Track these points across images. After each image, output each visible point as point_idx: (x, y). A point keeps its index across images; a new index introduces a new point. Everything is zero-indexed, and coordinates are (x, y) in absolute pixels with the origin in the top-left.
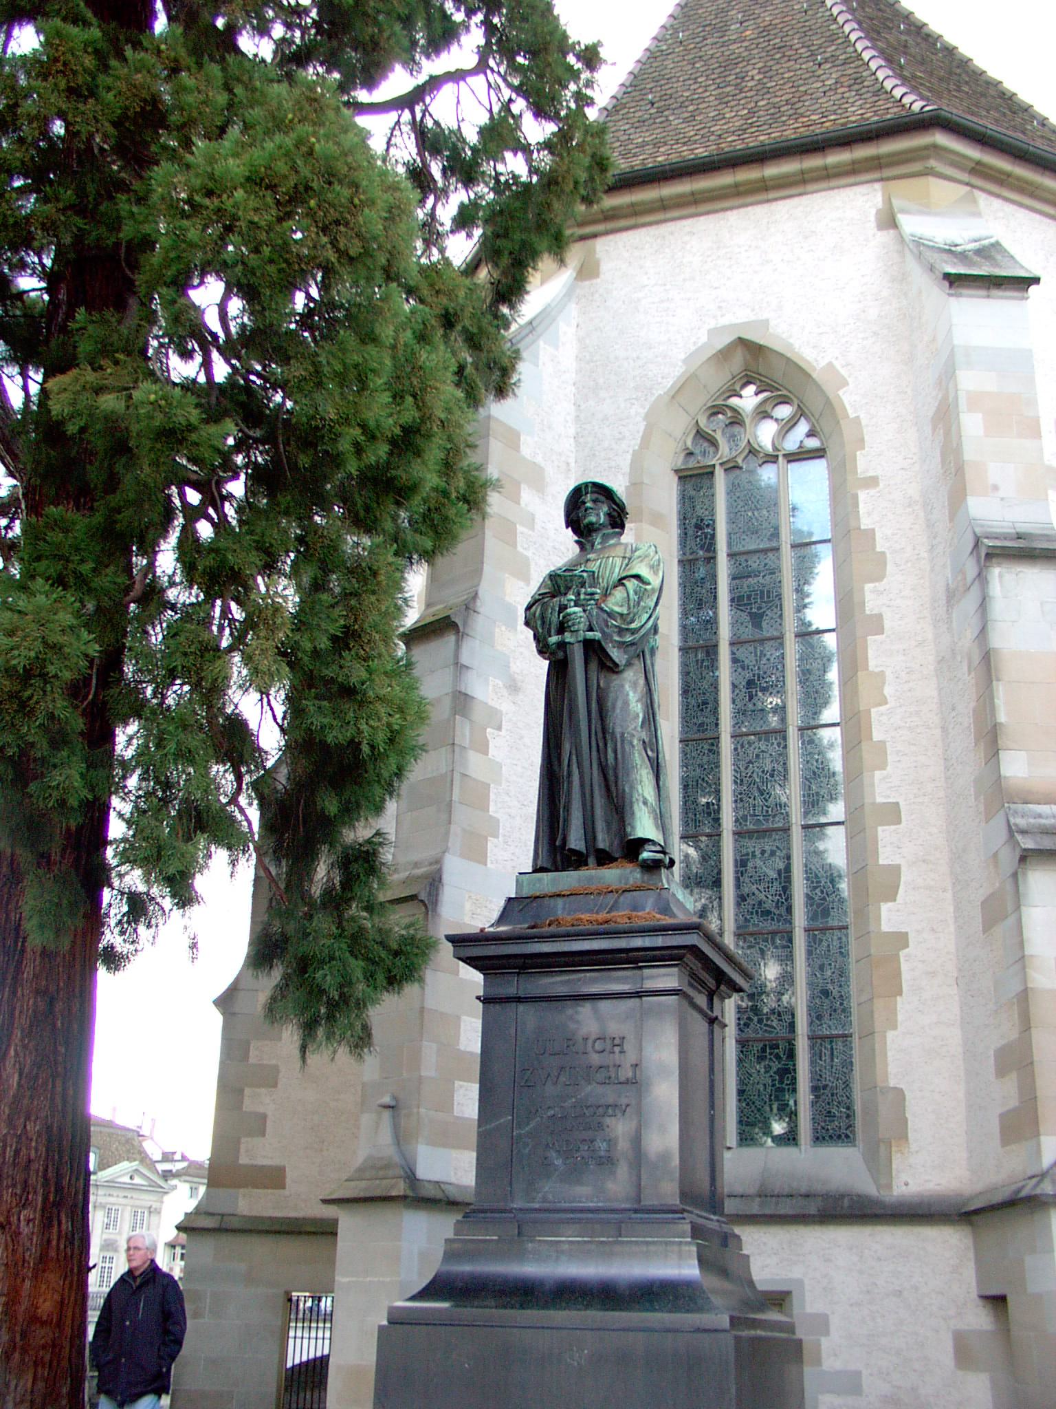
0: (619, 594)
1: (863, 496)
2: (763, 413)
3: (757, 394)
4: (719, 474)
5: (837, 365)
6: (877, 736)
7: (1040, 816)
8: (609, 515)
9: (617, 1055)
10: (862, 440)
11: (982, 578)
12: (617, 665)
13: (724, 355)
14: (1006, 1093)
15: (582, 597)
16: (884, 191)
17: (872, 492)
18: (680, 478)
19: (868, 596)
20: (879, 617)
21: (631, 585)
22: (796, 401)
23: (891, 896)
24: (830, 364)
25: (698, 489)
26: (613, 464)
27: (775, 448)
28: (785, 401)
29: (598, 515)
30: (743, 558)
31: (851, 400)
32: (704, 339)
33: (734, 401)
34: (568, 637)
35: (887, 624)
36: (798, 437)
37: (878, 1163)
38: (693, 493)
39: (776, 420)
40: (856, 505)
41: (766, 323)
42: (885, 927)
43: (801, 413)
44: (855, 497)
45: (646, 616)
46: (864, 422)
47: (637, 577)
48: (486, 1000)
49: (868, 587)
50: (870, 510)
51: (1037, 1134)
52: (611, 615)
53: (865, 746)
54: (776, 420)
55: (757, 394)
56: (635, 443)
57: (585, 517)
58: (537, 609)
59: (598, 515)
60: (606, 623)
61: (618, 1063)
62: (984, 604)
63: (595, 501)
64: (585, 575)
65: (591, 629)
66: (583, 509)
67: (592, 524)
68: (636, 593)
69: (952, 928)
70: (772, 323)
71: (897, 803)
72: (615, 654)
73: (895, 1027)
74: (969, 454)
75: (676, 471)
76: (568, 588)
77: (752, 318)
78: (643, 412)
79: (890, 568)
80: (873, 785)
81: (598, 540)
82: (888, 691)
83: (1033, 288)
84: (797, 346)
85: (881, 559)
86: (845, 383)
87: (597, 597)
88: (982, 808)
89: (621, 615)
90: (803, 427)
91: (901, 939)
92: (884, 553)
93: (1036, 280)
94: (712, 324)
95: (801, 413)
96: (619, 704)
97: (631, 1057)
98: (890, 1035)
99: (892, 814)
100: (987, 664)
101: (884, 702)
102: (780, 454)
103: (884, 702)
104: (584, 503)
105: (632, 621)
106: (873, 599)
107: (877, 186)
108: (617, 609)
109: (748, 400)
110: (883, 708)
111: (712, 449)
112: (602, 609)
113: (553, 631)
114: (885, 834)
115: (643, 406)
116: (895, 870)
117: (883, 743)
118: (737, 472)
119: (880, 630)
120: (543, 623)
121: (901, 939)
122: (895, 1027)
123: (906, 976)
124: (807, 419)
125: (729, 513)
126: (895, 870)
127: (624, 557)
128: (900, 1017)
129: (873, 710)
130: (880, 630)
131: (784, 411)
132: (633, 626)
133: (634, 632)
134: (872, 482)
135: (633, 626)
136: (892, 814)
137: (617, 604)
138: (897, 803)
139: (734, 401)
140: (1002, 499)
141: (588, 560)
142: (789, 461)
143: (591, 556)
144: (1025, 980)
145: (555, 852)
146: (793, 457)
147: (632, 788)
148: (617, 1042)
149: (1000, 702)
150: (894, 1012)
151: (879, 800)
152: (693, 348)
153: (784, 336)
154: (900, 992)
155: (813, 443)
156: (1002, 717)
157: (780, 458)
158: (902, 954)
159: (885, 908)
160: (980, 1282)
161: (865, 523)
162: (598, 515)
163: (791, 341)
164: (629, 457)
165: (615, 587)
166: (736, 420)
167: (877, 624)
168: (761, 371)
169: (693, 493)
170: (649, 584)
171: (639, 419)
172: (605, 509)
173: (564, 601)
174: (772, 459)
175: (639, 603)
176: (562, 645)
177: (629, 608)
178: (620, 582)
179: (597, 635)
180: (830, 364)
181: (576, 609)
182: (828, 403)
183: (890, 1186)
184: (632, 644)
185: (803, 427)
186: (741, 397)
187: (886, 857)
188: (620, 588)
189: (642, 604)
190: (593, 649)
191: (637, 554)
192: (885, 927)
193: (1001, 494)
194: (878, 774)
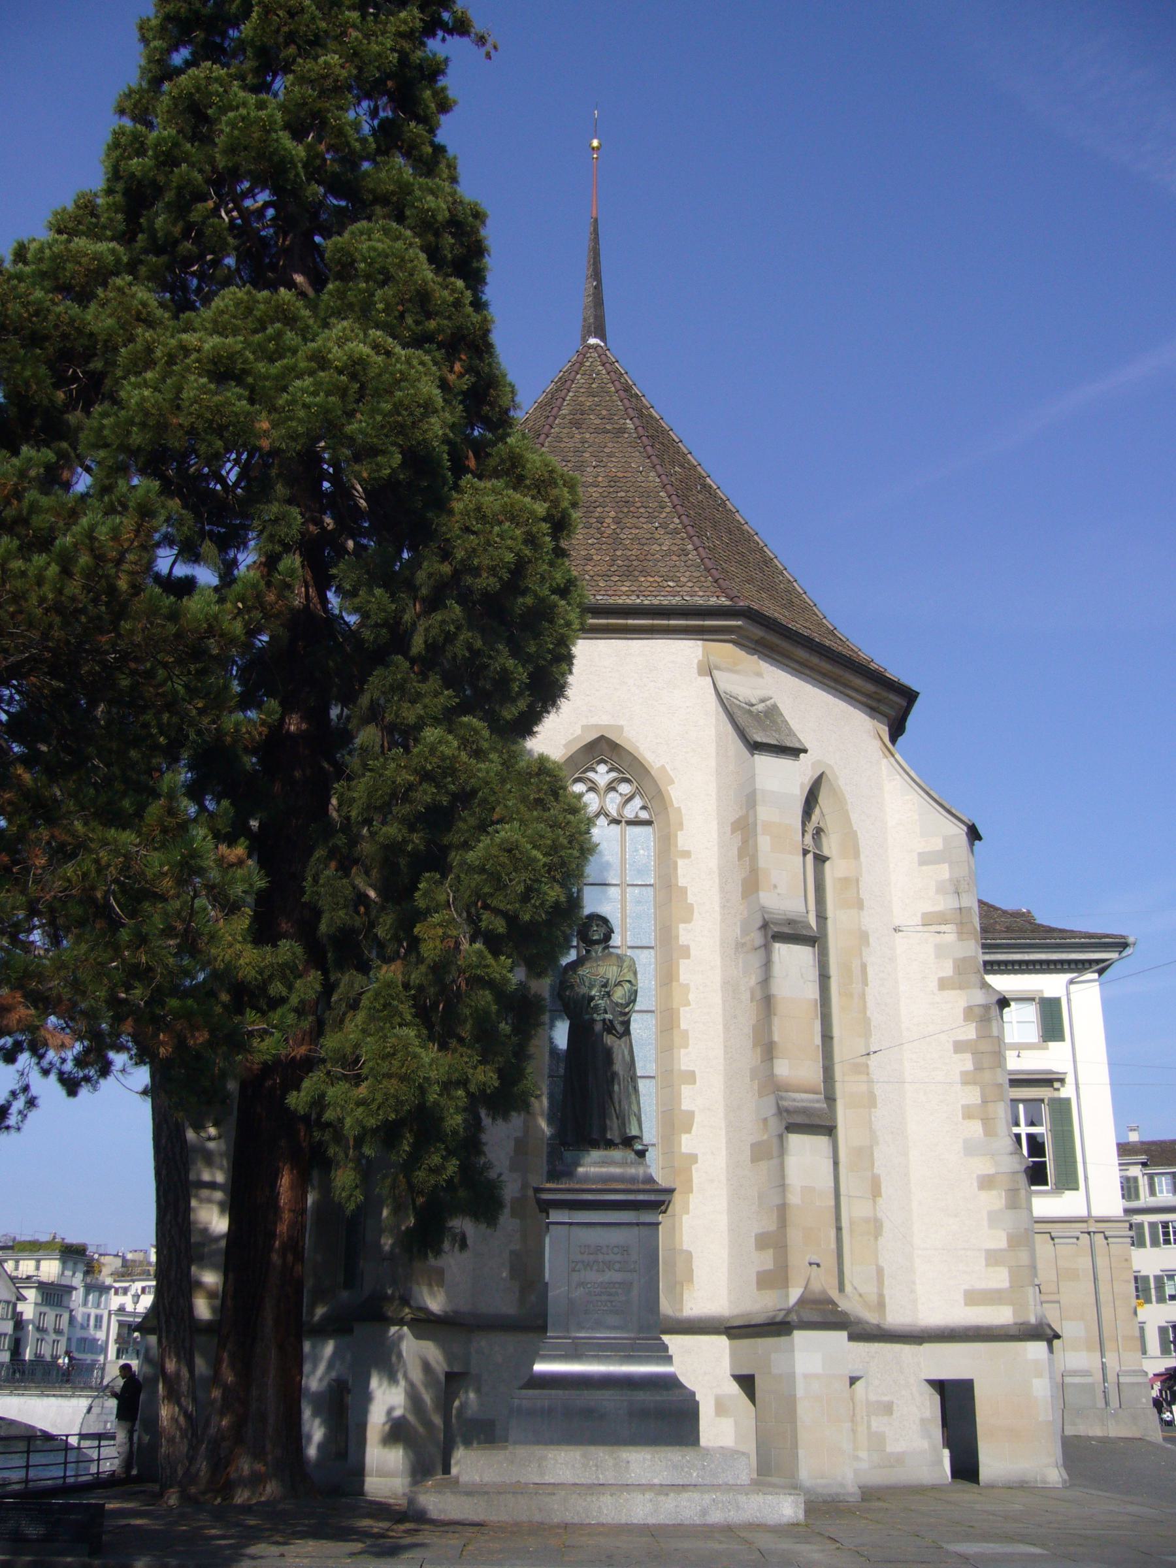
1: (681, 863)
5: (668, 768)
6: (683, 1026)
7: (794, 1100)
10: (681, 824)
11: (767, 948)
14: (766, 1261)
16: (704, 648)
17: (687, 861)
19: (681, 932)
20: (688, 948)
21: (627, 986)
23: (688, 1130)
24: (663, 766)
31: (676, 794)
35: (692, 952)
36: (633, 810)
40: (676, 868)
41: (621, 728)
42: (684, 1150)
43: (638, 792)
44: (676, 863)
46: (683, 811)
47: (629, 982)
49: (682, 926)
50: (685, 874)
51: (787, 1287)
53: (675, 1031)
62: (767, 965)
63: (597, 926)
69: (724, 1153)
70: (626, 729)
71: (693, 1072)
73: (688, 1213)
74: (762, 863)
77: (612, 723)
79: (696, 915)
80: (679, 1058)
82: (691, 997)
83: (802, 755)
85: (690, 909)
86: (672, 782)
88: (756, 1088)
91: (693, 1158)
92: (692, 904)
93: (805, 751)
94: (584, 722)
95: (638, 792)
96: (620, 1056)
98: (685, 1217)
99: (691, 1077)
100: (767, 1003)
101: (688, 1004)
103: (688, 1004)
106: (685, 934)
107: (700, 643)
110: (687, 1008)
114: (686, 1091)
116: (691, 1114)
117: (687, 1031)
119: (688, 957)
121: (693, 1158)
122: (688, 1213)
123: (695, 1181)
124: (642, 797)
126: (691, 1114)
128: (691, 1207)
129: (682, 1009)
130: (688, 957)
131: (625, 788)
134: (687, 854)
136: (691, 1077)
138: (693, 1072)
139: (591, 775)
144: (784, 1197)
146: (630, 823)
147: (630, 1107)
149: (775, 1029)
150: (687, 1203)
151: (683, 1068)
154: (692, 1192)
155: (644, 815)
156: (776, 1038)
158: (694, 1167)
159: (685, 1138)
160: (732, 1369)
161: (682, 882)
167: (686, 952)
174: (618, 822)
180: (663, 766)
182: (660, 792)
183: (682, 1310)
185: (637, 802)
187: (685, 1105)
192: (684, 1150)
194: (683, 1051)
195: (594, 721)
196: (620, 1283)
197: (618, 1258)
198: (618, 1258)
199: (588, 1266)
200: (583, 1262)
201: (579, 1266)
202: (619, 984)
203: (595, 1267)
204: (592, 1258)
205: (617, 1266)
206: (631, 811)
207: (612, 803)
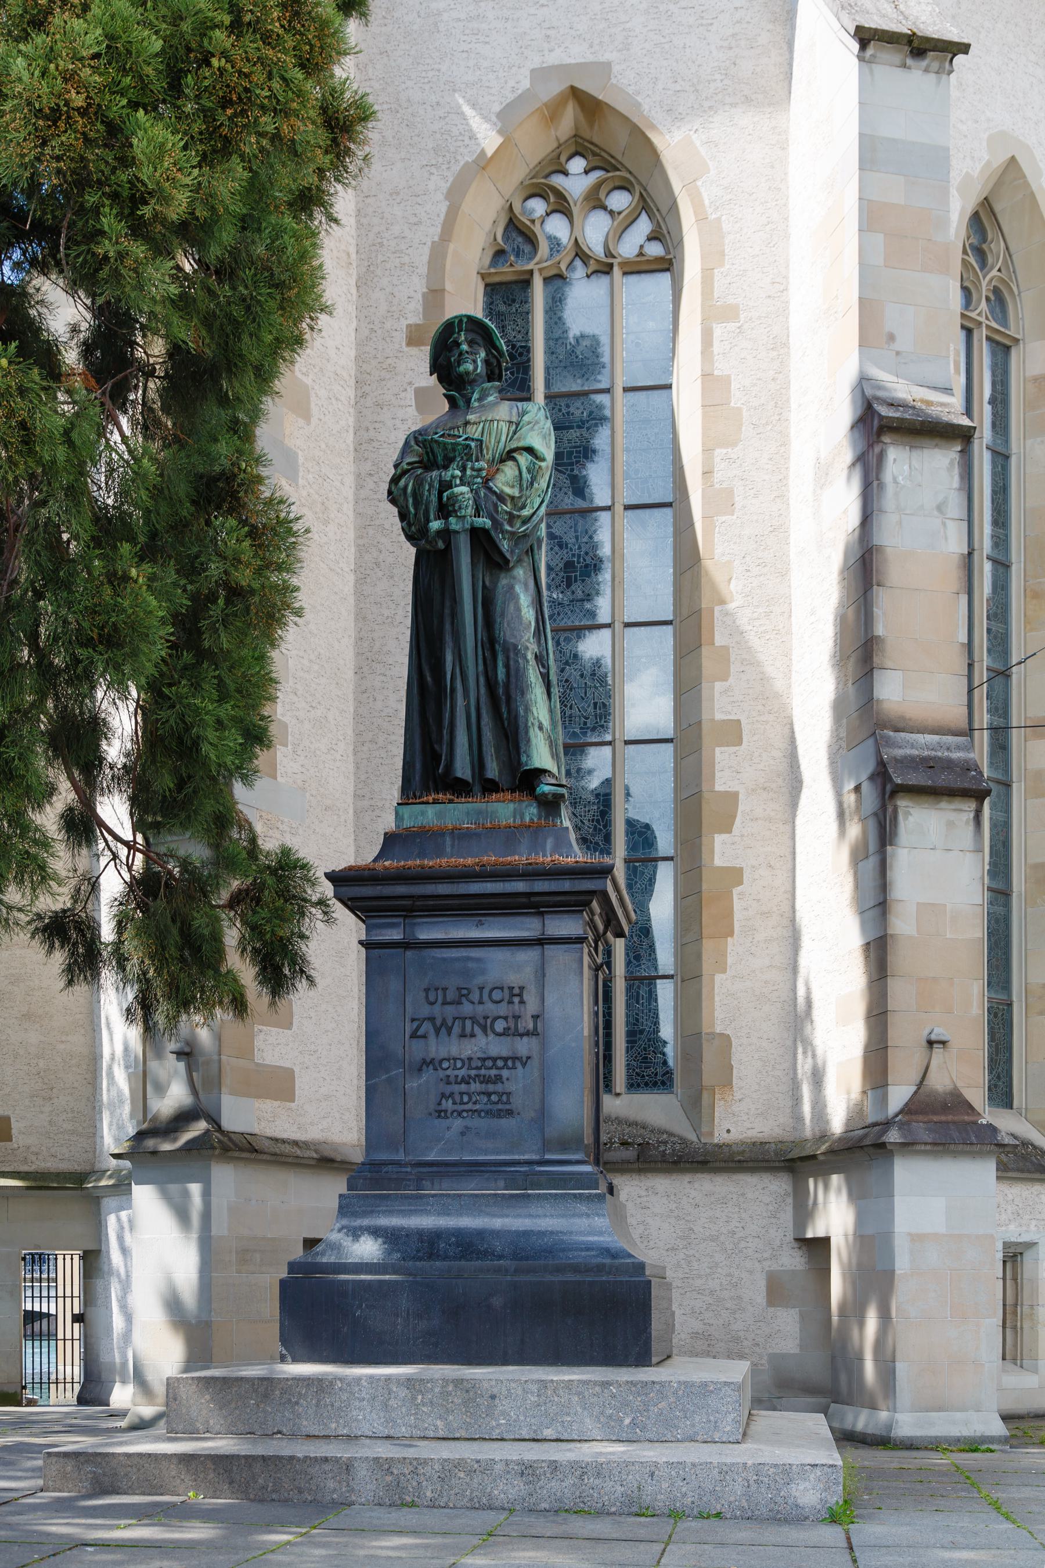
0: (509, 471)
2: (595, 201)
3: (586, 172)
4: (538, 283)
8: (487, 362)
9: (517, 1006)
10: (722, 254)
12: (507, 561)
13: (552, 112)
15: (469, 472)
18: (486, 285)
22: (637, 187)
25: (510, 301)
26: (406, 260)
27: (609, 254)
28: (624, 187)
29: (475, 361)
30: (563, 402)
32: (526, 84)
33: (558, 180)
34: (454, 524)
37: (696, 1106)
38: (502, 308)
39: (611, 213)
41: (606, 67)
45: (538, 500)
46: (726, 227)
48: (366, 944)
52: (501, 497)
54: (611, 213)
55: (586, 172)
56: (434, 232)
57: (459, 365)
58: (408, 483)
59: (475, 363)
60: (496, 506)
61: (517, 1014)
63: (471, 343)
64: (473, 444)
65: (477, 514)
66: (456, 353)
67: (467, 373)
68: (529, 471)
70: (616, 69)
72: (505, 545)
75: (483, 276)
76: (452, 460)
77: (591, 58)
78: (445, 186)
81: (476, 396)
84: (646, 107)
87: (484, 473)
89: (513, 498)
90: (643, 226)
94: (535, 62)
96: (512, 607)
97: (532, 1006)
102: (615, 261)
104: (458, 345)
105: (524, 507)
108: (508, 490)
109: (577, 180)
111: (527, 248)
112: (490, 489)
113: (432, 516)
115: (444, 178)
118: (559, 282)
120: (416, 504)
125: (547, 339)
127: (511, 422)
131: (619, 201)
132: (526, 512)
133: (526, 521)
135: (526, 512)
137: (508, 484)
139: (558, 180)
140: (898, 353)
141: (467, 423)
142: (625, 273)
143: (471, 417)
145: (428, 770)
148: (516, 991)
152: (511, 97)
153: (630, 90)
155: (655, 250)
157: (616, 269)
162: (475, 363)
163: (639, 99)
164: (426, 251)
165: (502, 461)
166: (561, 205)
168: (595, 140)
169: (502, 308)
170: (543, 460)
171: (440, 196)
172: (483, 354)
173: (447, 475)
174: (606, 269)
175: (532, 484)
176: (446, 534)
177: (521, 490)
178: (509, 456)
179: (484, 522)
181: (464, 489)
184: (525, 536)
185: (643, 226)
186: (566, 173)
188: (510, 463)
189: (536, 485)
190: (483, 542)
191: (526, 418)
193: (897, 346)
195: (555, 58)
196: (505, 1059)
197: (503, 1009)
198: (503, 1009)
199: (443, 1028)
200: (432, 1019)
201: (427, 1027)
202: (509, 456)
203: (456, 1029)
204: (450, 1011)
205: (500, 1026)
206: (629, 247)
207: (595, 231)
